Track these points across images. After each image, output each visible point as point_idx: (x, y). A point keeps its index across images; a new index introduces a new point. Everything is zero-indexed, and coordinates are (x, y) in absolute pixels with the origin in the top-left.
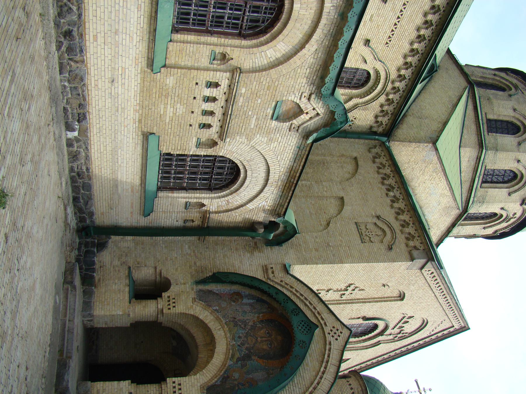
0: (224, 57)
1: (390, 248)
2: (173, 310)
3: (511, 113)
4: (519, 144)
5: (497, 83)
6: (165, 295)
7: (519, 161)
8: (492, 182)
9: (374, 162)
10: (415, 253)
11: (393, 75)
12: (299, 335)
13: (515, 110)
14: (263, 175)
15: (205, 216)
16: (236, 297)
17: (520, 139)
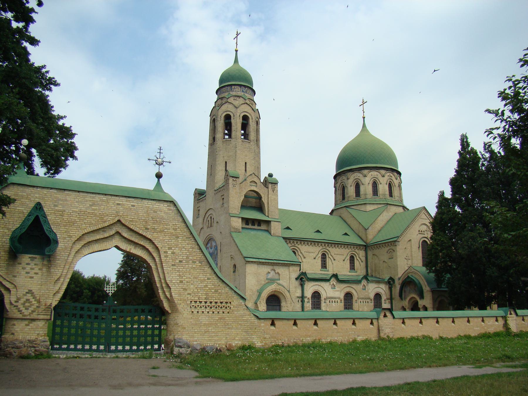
0: (356, 301)
1: (394, 251)
2: (408, 306)
3: (352, 187)
4: (363, 184)
5: (341, 189)
6: (405, 307)
7: (369, 184)
8: (377, 191)
9: (373, 250)
10: (395, 245)
11: (350, 250)
12: (409, 280)
13: (351, 186)
14: (377, 288)
15: (388, 299)
16: (405, 291)
17: (361, 183)
